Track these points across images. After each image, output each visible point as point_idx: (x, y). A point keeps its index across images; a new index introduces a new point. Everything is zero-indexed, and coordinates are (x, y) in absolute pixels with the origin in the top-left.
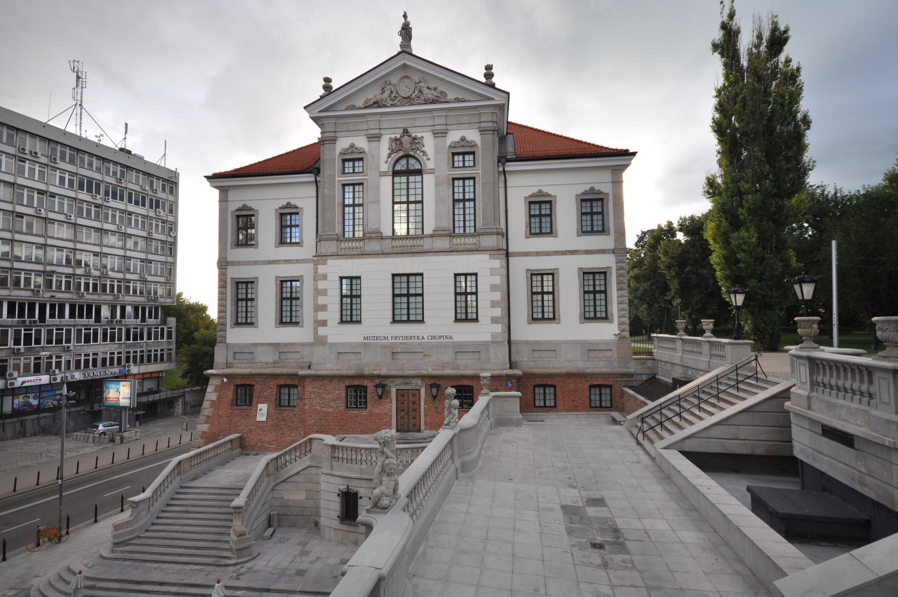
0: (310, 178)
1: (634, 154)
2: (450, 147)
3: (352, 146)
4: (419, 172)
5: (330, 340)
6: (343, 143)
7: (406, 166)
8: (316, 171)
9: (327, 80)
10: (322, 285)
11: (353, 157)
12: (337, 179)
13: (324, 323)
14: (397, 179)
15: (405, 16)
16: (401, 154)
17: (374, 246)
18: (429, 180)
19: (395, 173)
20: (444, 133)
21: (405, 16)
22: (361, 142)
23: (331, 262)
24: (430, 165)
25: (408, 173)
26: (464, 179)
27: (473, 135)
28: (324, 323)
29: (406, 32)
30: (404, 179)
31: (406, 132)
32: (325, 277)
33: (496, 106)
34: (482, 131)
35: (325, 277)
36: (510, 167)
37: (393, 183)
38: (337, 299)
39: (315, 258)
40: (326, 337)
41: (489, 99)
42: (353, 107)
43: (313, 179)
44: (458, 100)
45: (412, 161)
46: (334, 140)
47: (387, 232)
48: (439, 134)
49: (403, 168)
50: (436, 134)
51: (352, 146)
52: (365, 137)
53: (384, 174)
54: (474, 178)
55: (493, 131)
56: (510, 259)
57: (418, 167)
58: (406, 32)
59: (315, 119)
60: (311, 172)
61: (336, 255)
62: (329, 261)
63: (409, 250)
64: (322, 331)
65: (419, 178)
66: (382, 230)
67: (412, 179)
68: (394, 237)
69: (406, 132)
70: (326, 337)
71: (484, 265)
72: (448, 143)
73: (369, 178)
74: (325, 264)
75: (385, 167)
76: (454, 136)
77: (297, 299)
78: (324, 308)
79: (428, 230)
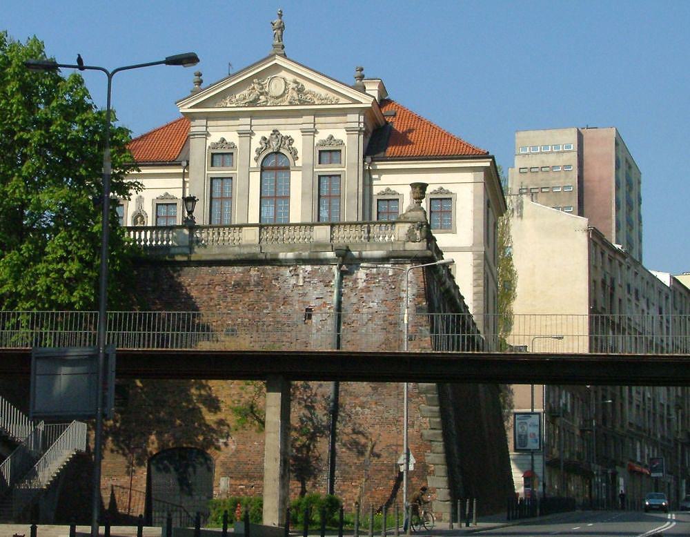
3: (223, 140)
6: (215, 138)
7: (275, 163)
8: (184, 164)
11: (222, 155)
12: (207, 172)
16: (271, 151)
22: (232, 137)
25: (277, 169)
27: (340, 134)
34: (348, 130)
46: (207, 135)
50: (304, 132)
52: (236, 133)
55: (359, 131)
69: (275, 131)
73: (237, 172)
76: (323, 135)
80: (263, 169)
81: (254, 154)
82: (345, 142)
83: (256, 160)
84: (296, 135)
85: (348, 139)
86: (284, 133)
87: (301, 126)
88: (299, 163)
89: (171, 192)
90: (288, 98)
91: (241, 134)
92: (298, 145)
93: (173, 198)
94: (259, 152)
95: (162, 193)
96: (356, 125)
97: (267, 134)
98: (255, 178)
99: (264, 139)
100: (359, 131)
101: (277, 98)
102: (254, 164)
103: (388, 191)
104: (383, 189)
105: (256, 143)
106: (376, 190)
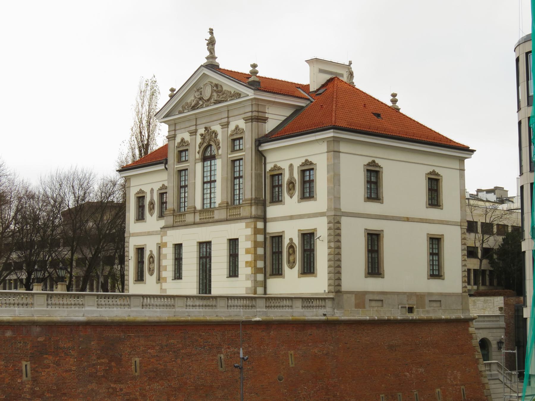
8: (165, 162)
9: (172, 90)
12: (176, 166)
14: (206, 163)
15: (211, 32)
16: (205, 144)
17: (189, 218)
19: (204, 159)
20: (228, 124)
21: (211, 32)
22: (187, 137)
23: (170, 232)
26: (239, 160)
27: (242, 124)
29: (211, 43)
30: (209, 162)
33: (252, 99)
34: (246, 120)
36: (265, 147)
37: (204, 167)
39: (163, 230)
43: (163, 167)
47: (199, 207)
49: (209, 155)
56: (268, 224)
58: (211, 43)
59: (165, 122)
60: (162, 163)
61: (173, 227)
67: (213, 161)
71: (242, 231)
72: (229, 133)
75: (198, 156)
76: (232, 127)
80: (204, 159)
81: (197, 149)
83: (198, 153)
84: (216, 128)
85: (246, 126)
87: (219, 122)
88: (220, 152)
90: (212, 101)
92: (220, 137)
96: (250, 114)
97: (202, 131)
98: (199, 166)
99: (202, 135)
100: (252, 119)
101: (208, 100)
103: (276, 168)
105: (199, 140)
106: (269, 167)
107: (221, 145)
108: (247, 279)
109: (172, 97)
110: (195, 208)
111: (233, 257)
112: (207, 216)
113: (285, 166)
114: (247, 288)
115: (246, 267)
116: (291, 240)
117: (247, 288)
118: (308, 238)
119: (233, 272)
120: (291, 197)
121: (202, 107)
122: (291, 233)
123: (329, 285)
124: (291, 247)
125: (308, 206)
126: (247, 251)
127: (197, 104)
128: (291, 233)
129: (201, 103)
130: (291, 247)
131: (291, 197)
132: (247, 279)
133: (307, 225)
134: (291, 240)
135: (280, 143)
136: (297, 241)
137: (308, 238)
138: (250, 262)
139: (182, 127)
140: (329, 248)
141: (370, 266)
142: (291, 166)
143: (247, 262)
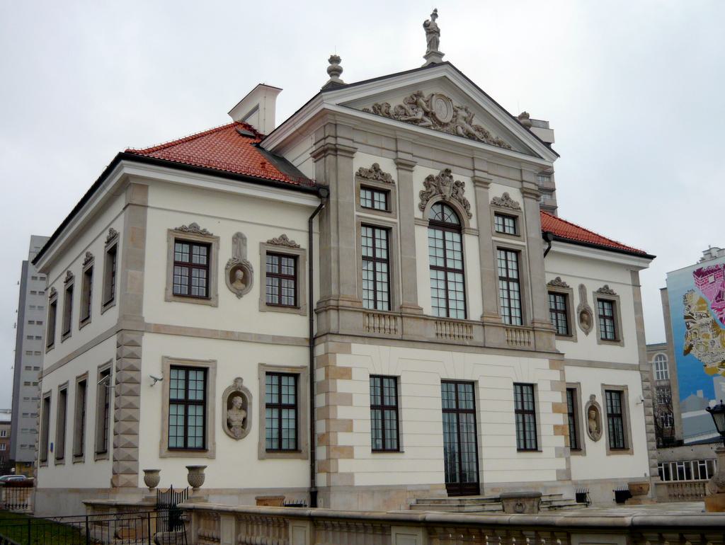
0: (311, 201)
1: (652, 257)
2: (495, 203)
4: (459, 229)
5: (359, 481)
6: (363, 161)
10: (342, 386)
13: (348, 452)
16: (439, 198)
17: (413, 328)
18: (471, 242)
22: (387, 166)
23: (357, 347)
24: (472, 223)
27: (515, 196)
28: (348, 452)
29: (432, 31)
30: (439, 234)
31: (448, 171)
32: (346, 373)
34: (525, 193)
35: (346, 373)
38: (367, 413)
40: (351, 475)
41: (532, 153)
42: (377, 111)
44: (499, 144)
45: (447, 211)
47: (428, 311)
48: (480, 183)
49: (437, 218)
50: (477, 182)
51: (376, 168)
53: (417, 222)
54: (517, 252)
57: (453, 220)
58: (432, 31)
62: (353, 345)
63: (456, 341)
64: (344, 465)
65: (456, 237)
66: (420, 304)
67: (449, 235)
68: (466, 323)
70: (351, 475)
74: (348, 351)
76: (496, 190)
77: (269, 406)
78: (348, 426)
79: (475, 314)
81: (417, 200)
82: (521, 206)
83: (422, 208)
86: (456, 178)
89: (291, 237)
91: (400, 165)
93: (293, 246)
94: (425, 196)
95: (275, 234)
96: (533, 187)
98: (423, 236)
102: (418, 214)
104: (553, 278)
107: (472, 210)
108: (558, 455)
109: (335, 71)
110: (422, 309)
111: (526, 412)
112: (453, 330)
113: (573, 284)
114: (558, 471)
115: (555, 434)
116: (593, 397)
117: (558, 471)
118: (617, 395)
119: (528, 442)
120: (587, 334)
121: (428, 127)
122: (592, 387)
123: (651, 467)
124: (593, 408)
125: (610, 352)
126: (556, 409)
127: (422, 120)
128: (592, 387)
129: (429, 121)
130: (593, 408)
131: (587, 334)
132: (558, 455)
133: (616, 379)
134: (593, 397)
135: (569, 248)
136: (600, 400)
137: (617, 395)
138: (563, 427)
139: (370, 143)
140: (647, 415)
141: (612, 438)
142: (582, 287)
143: (556, 427)
